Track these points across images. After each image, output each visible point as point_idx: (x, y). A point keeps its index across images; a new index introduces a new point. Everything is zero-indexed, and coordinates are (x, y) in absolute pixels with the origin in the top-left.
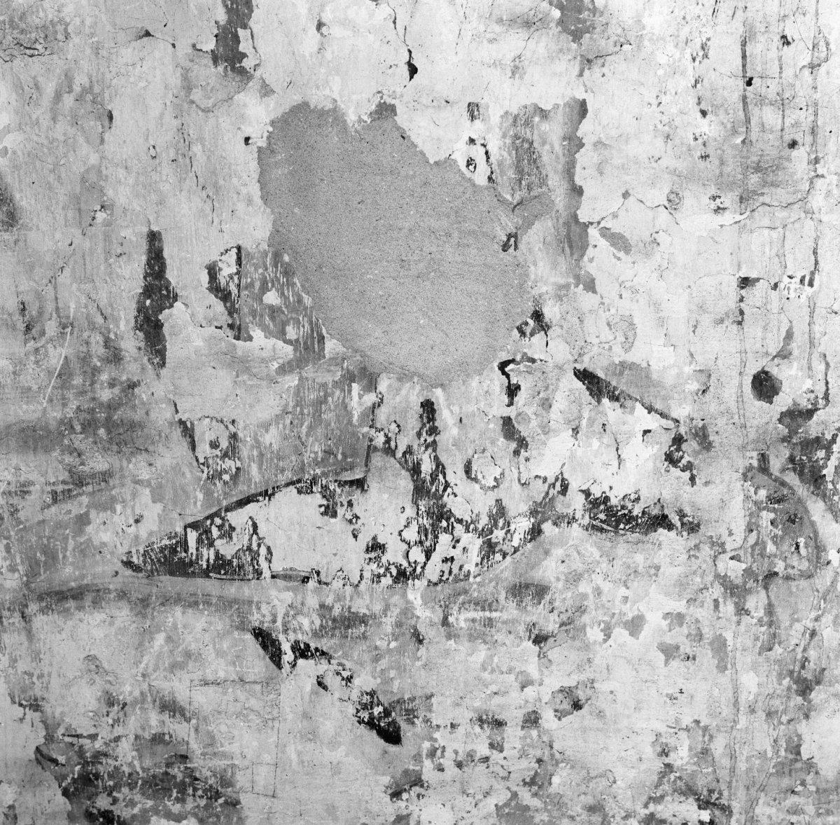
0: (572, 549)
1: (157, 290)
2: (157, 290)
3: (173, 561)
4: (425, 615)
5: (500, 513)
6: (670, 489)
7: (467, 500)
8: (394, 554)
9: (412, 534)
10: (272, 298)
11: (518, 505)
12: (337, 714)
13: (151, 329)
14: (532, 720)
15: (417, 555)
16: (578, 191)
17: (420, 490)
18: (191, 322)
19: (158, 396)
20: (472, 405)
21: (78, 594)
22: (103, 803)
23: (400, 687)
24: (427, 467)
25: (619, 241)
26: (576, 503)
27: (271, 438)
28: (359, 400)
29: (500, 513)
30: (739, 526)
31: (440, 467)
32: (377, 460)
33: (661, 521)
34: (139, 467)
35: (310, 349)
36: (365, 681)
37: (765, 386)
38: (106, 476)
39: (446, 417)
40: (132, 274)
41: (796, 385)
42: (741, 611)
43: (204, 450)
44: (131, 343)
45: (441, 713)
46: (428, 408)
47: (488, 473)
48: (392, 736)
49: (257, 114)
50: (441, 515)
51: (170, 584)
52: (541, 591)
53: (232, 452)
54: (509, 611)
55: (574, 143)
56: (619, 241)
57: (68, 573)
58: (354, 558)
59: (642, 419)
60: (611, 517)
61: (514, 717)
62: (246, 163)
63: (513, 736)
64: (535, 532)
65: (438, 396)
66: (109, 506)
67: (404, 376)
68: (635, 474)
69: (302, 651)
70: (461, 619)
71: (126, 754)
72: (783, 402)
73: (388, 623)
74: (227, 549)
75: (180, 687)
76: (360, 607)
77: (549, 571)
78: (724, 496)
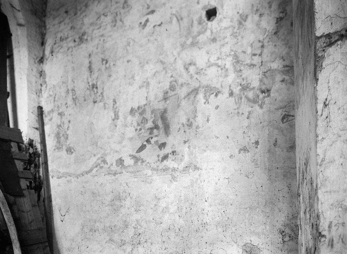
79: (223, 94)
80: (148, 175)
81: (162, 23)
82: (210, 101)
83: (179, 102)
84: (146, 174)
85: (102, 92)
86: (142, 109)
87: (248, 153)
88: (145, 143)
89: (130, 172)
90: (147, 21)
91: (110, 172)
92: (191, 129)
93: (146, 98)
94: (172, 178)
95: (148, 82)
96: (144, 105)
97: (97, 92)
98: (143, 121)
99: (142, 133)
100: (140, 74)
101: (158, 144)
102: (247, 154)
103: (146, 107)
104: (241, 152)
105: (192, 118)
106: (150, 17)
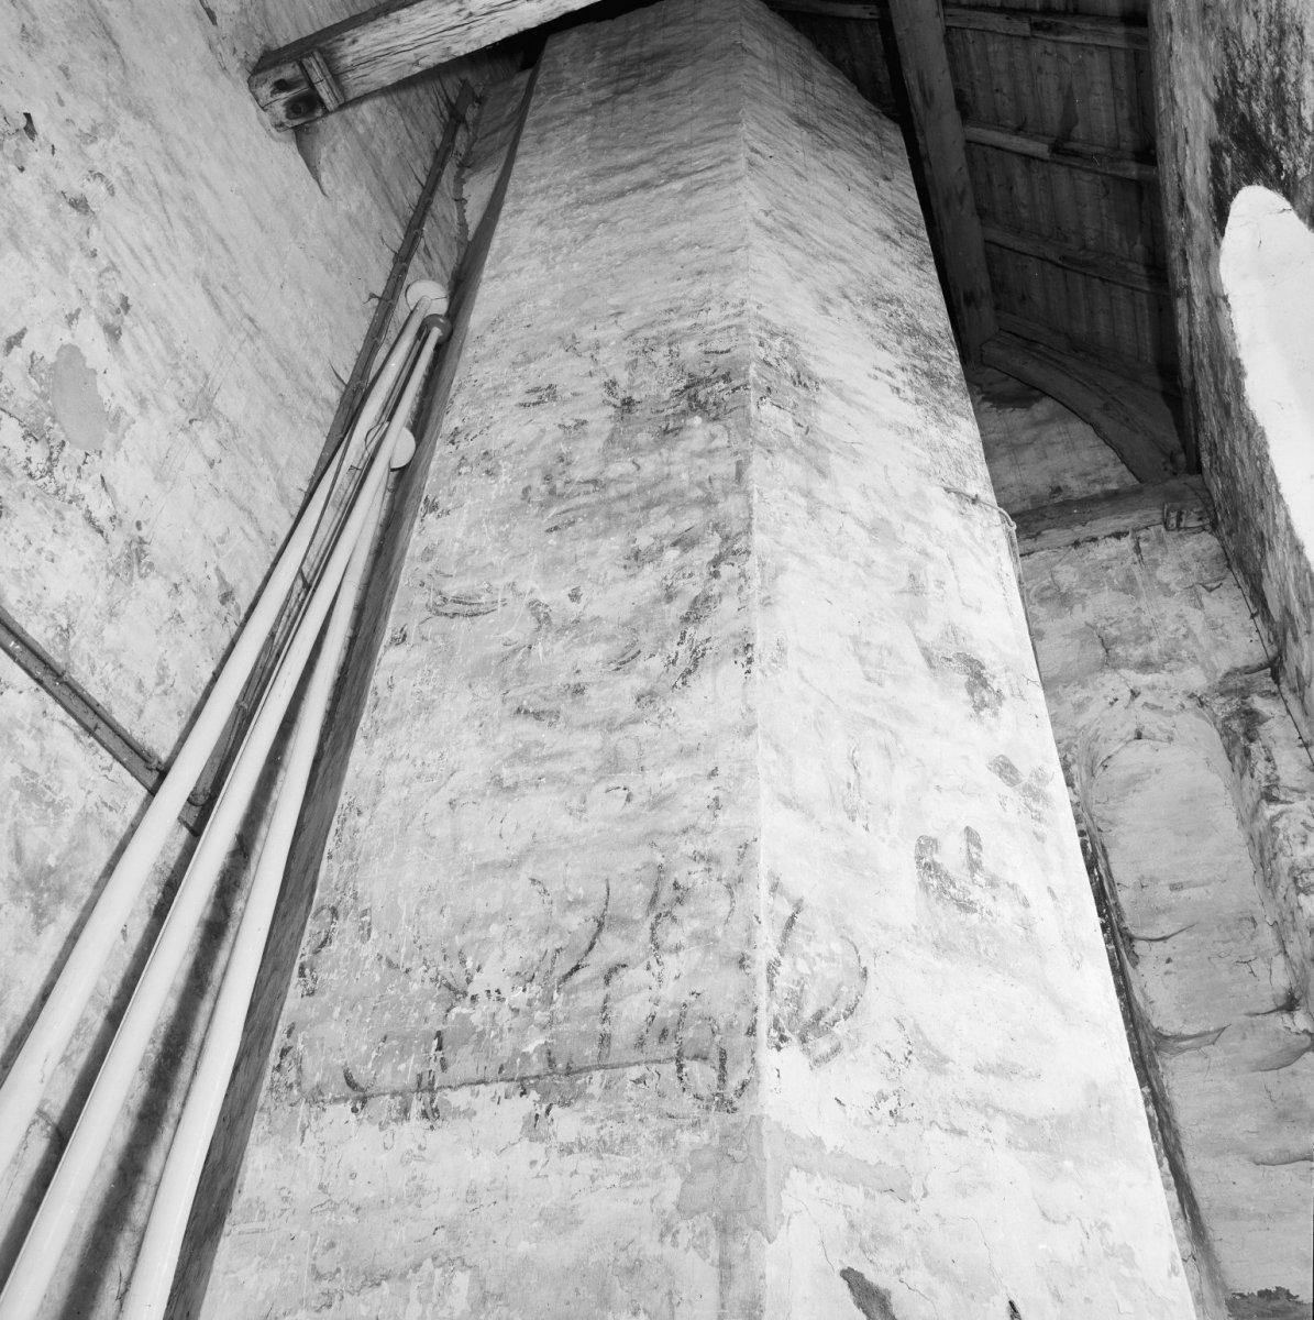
0: (74, 515)
4: (30, 494)
5: (65, 487)
6: (107, 526)
7: (57, 472)
8: (32, 467)
9: (41, 467)
14: (39, 551)
15: (38, 474)
16: (124, 436)
17: (49, 459)
20: (72, 454)
24: (54, 456)
27: (22, 404)
32: (44, 440)
33: (102, 532)
35: (44, 396)
37: (138, 525)
39: (67, 449)
40: (13, 330)
41: (144, 533)
45: (16, 523)
46: (63, 443)
49: (67, 339)
50: (50, 472)
52: (63, 519)
53: (10, 394)
54: (52, 514)
58: (22, 457)
60: (90, 520)
61: (36, 544)
62: (57, 345)
63: (32, 550)
64: (70, 502)
65: (67, 443)
67: (62, 429)
68: (101, 514)
70: (39, 504)
72: (141, 534)
73: (19, 483)
76: (14, 471)
77: (68, 515)
78: (119, 539)
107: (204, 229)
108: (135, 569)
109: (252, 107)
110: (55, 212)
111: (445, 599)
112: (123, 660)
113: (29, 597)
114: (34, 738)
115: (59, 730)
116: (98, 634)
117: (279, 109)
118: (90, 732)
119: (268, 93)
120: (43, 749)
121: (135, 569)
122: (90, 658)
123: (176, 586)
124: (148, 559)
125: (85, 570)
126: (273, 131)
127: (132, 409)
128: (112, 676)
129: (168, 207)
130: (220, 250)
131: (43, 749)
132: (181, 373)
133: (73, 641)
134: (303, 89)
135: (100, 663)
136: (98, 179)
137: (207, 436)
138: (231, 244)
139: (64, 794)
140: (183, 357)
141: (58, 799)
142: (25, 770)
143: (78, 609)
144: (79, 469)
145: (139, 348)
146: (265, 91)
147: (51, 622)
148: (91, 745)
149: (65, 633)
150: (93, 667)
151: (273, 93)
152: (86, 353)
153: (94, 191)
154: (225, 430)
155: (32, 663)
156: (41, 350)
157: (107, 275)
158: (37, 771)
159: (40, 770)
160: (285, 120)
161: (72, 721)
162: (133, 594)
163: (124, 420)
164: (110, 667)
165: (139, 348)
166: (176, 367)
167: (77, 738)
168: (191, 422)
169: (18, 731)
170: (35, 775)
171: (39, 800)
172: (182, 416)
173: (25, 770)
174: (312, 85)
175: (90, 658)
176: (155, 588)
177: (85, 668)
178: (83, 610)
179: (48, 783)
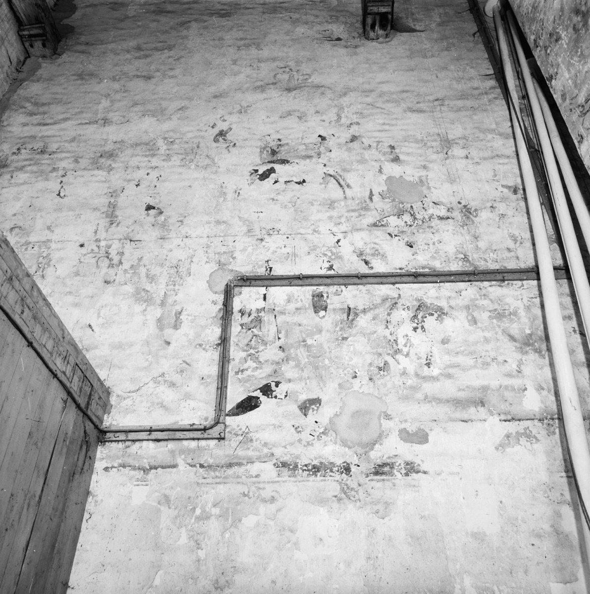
0: (435, 222)
1: (371, 194)
2: (371, 194)
3: (375, 225)
4: (415, 231)
5: (424, 218)
6: (449, 214)
7: (418, 216)
8: (409, 223)
9: (411, 220)
10: (388, 195)
11: (427, 217)
12: (402, 244)
13: (371, 199)
14: (434, 244)
15: (412, 223)
17: (412, 215)
18: (376, 198)
19: (371, 205)
20: (417, 206)
21: (360, 229)
22: (364, 258)
23: (412, 240)
24: (412, 213)
25: (435, 188)
26: (435, 216)
27: (389, 210)
28: (401, 206)
29: (424, 218)
30: (460, 219)
31: (414, 213)
33: (449, 218)
34: (369, 213)
35: (394, 200)
36: (406, 239)
37: (459, 203)
38: (364, 215)
39: (414, 207)
40: (368, 193)
41: (463, 203)
42: (463, 229)
43: (379, 211)
44: (368, 200)
45: (419, 243)
46: (412, 207)
47: (422, 213)
48: (411, 247)
49: (385, 177)
50: (415, 218)
51: (374, 228)
52: (432, 227)
54: (428, 229)
55: (427, 179)
56: (435, 188)
57: (358, 227)
58: (403, 224)
59: (443, 207)
60: (441, 218)
61: (431, 242)
62: (383, 182)
63: (431, 246)
64: (430, 220)
65: (413, 205)
66: (365, 218)
67: (407, 203)
68: (443, 212)
69: (396, 236)
70: (420, 231)
71: (368, 251)
72: (463, 204)
73: (409, 231)
74: (383, 223)
75: (377, 241)
77: (433, 224)
78: (457, 214)
79: (454, 319)
80: (263, 477)
81: (304, 181)
82: (426, 325)
83: (350, 318)
84: (257, 476)
85: (135, 264)
86: (252, 317)
87: (536, 443)
88: (258, 394)
89: (202, 466)
90: (272, 170)
91: (130, 461)
92: (388, 378)
93: (262, 296)
94: (343, 490)
95: (271, 268)
96: (259, 311)
97: (121, 263)
98: (253, 343)
99: (247, 370)
100: (250, 249)
101: (296, 401)
102: (536, 446)
103: (262, 314)
104: (520, 438)
105: (389, 354)
106: (277, 167)
107: (395, 96)
108: (471, 216)
109: (374, 44)
110: (349, 150)
111: (583, 106)
112: (494, 248)
113: (443, 260)
114: (485, 299)
115: (491, 289)
116: (477, 248)
117: (381, 32)
118: (503, 280)
119: (373, 33)
120: (491, 300)
121: (471, 216)
122: (481, 258)
123: (492, 207)
124: (473, 209)
125: (454, 234)
126: (387, 40)
127: (423, 173)
128: (495, 256)
129: (378, 106)
130: (405, 95)
131: (491, 300)
132: (429, 144)
133: (470, 259)
134: (378, 18)
135: (486, 256)
136: (352, 126)
137: (457, 151)
138: (407, 88)
139: (512, 308)
140: (425, 139)
141: (511, 310)
142: (490, 311)
143: (463, 247)
144: (423, 208)
145: (408, 154)
146: (372, 34)
147: (457, 260)
148: (508, 284)
149: (466, 259)
150: (485, 260)
151: (374, 31)
152: (393, 175)
153: (354, 130)
154: (461, 142)
155: (462, 278)
156: (380, 189)
157: (379, 147)
158: (495, 308)
159: (496, 306)
160: (386, 32)
161: (494, 283)
162: (478, 225)
163: (424, 179)
164: (491, 254)
165: (408, 154)
166: (425, 144)
167: (500, 286)
168: (447, 154)
169: (477, 302)
170: (496, 310)
171: (505, 316)
172: (442, 156)
173: (490, 311)
174: (378, 14)
175: (481, 258)
176: (484, 215)
177: (483, 263)
178: (465, 246)
179: (503, 309)
